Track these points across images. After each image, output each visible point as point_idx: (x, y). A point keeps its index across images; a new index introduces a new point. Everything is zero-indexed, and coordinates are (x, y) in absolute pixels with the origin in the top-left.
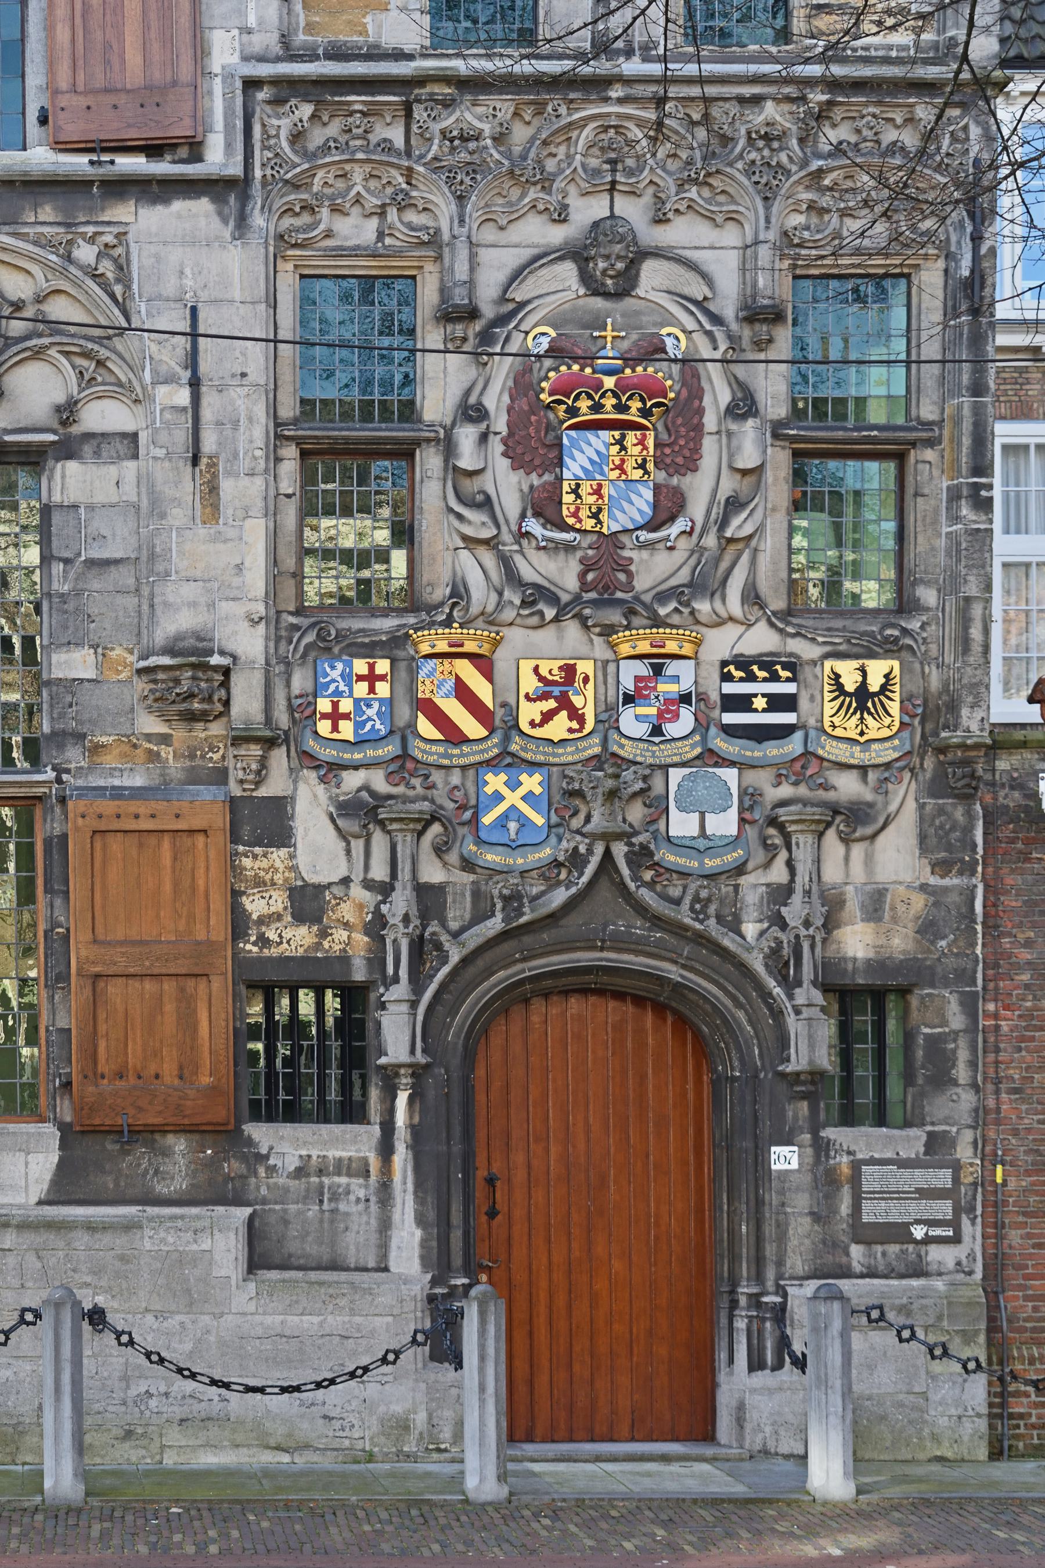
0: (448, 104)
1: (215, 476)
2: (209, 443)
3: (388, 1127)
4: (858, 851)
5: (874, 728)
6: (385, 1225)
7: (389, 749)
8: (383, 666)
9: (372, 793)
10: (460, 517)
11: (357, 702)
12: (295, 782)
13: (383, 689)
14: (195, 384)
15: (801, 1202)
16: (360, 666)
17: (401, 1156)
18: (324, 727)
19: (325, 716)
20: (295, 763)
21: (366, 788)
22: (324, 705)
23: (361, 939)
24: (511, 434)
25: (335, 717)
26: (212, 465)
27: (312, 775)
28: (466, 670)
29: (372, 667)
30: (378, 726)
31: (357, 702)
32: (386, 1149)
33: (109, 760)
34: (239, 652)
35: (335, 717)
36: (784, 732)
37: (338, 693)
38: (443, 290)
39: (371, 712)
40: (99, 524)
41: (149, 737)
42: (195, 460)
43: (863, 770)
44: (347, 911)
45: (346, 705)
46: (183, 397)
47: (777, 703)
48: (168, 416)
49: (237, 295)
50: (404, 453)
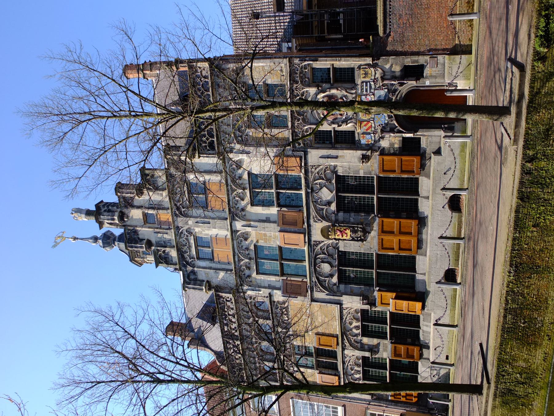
3: (421, 135)
4: (386, 74)
5: (370, 72)
6: (435, 136)
7: (372, 135)
15: (433, 80)
17: (425, 134)
22: (367, 143)
23: (397, 138)
28: (362, 125)
32: (424, 136)
33: (374, 169)
35: (368, 141)
36: (370, 85)
43: (375, 73)
44: (393, 140)
47: (366, 85)
50: (335, 131)
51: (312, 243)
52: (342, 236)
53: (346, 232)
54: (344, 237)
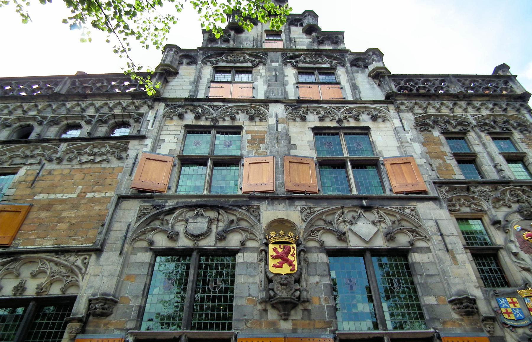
0: (476, 187)
1: (454, 254)
2: (450, 247)
8: (515, 300)
9: (527, 335)
10: (519, 263)
11: (512, 309)
12: (504, 332)
13: (518, 305)
14: (442, 235)
16: (509, 300)
18: (506, 316)
19: (505, 313)
20: (502, 327)
21: (524, 333)
22: (503, 310)
24: (521, 246)
25: (507, 313)
26: (452, 251)
27: (508, 330)
29: (512, 300)
30: (521, 315)
31: (512, 309)
34: (476, 295)
37: (505, 307)
38: (490, 219)
39: (517, 311)
40: (427, 266)
41: (457, 319)
42: (448, 250)
45: (509, 310)
46: (440, 238)
48: (438, 242)
49: (445, 218)
51: (255, 203)
52: (274, 257)
53: (285, 265)
54: (271, 262)
